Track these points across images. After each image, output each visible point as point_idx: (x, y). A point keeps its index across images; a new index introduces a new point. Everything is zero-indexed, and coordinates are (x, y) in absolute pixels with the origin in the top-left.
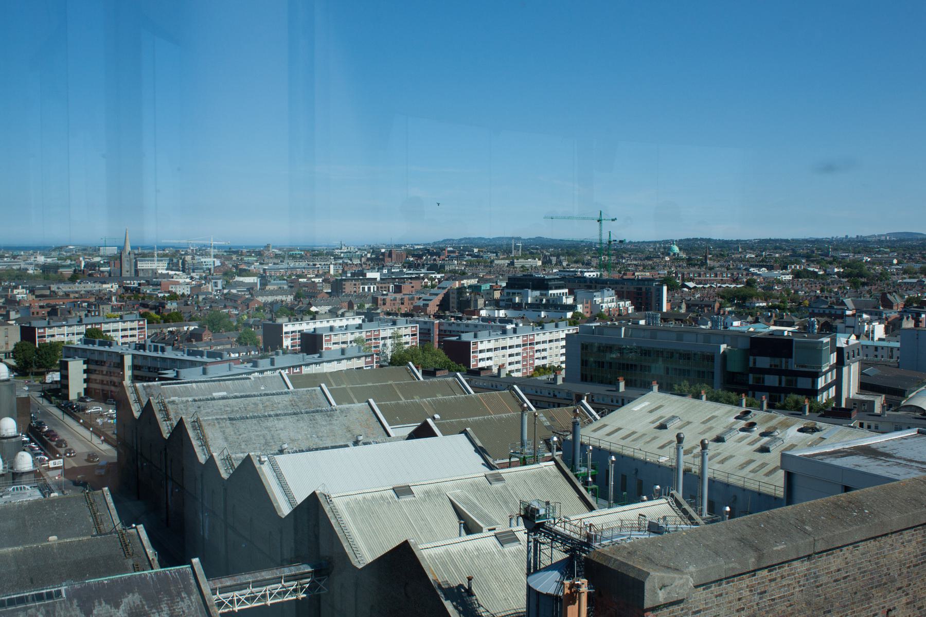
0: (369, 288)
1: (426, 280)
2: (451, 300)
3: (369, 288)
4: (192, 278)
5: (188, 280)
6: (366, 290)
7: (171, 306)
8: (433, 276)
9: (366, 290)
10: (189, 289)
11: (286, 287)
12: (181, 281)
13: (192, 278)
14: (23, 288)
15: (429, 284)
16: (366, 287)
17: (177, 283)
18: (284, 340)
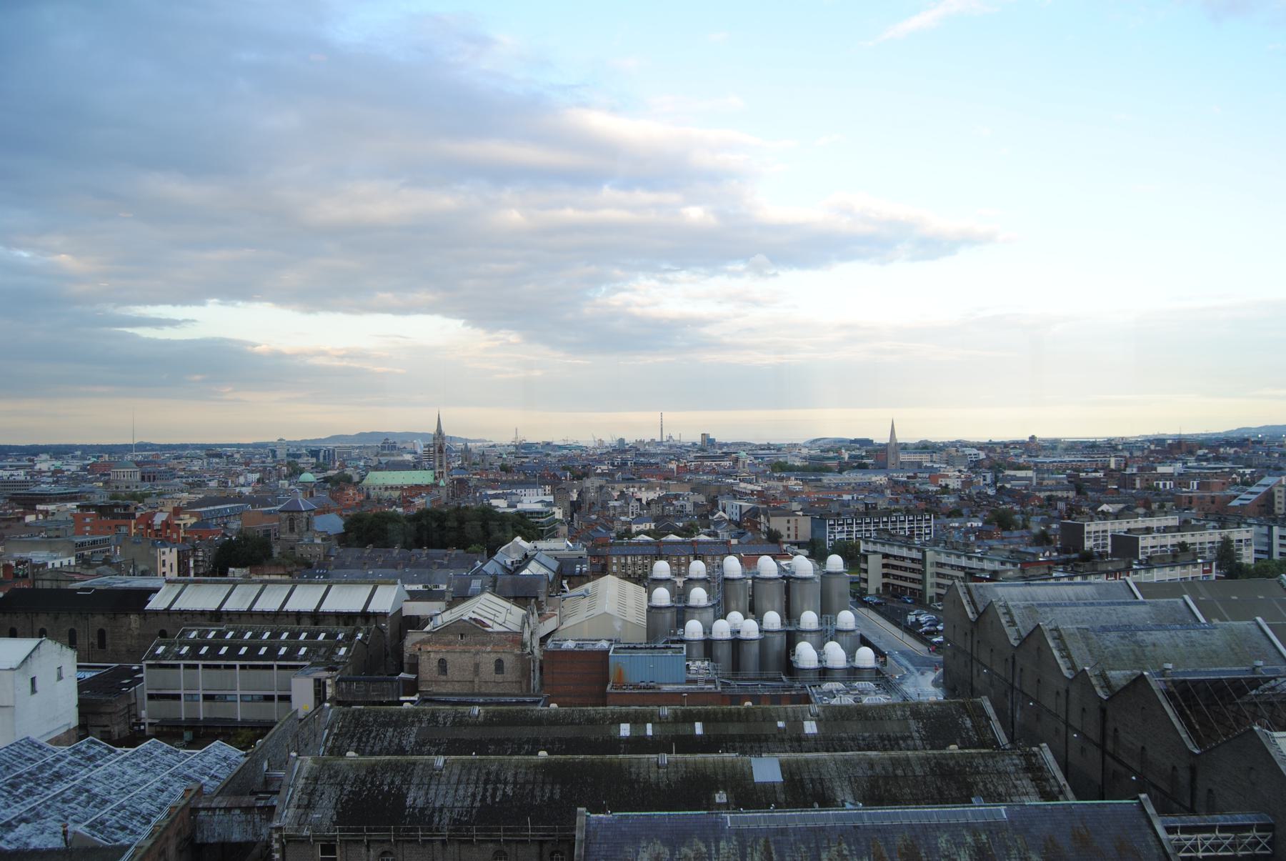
0: (1165, 485)
1: (1234, 476)
2: (1277, 500)
3: (1165, 485)
4: (960, 471)
5: (957, 473)
6: (1161, 486)
7: (950, 501)
8: (1241, 471)
9: (1161, 486)
10: (960, 483)
11: (1066, 482)
12: (950, 474)
13: (960, 471)
14: (796, 479)
15: (1239, 480)
16: (1161, 483)
17: (947, 476)
18: (1085, 539)
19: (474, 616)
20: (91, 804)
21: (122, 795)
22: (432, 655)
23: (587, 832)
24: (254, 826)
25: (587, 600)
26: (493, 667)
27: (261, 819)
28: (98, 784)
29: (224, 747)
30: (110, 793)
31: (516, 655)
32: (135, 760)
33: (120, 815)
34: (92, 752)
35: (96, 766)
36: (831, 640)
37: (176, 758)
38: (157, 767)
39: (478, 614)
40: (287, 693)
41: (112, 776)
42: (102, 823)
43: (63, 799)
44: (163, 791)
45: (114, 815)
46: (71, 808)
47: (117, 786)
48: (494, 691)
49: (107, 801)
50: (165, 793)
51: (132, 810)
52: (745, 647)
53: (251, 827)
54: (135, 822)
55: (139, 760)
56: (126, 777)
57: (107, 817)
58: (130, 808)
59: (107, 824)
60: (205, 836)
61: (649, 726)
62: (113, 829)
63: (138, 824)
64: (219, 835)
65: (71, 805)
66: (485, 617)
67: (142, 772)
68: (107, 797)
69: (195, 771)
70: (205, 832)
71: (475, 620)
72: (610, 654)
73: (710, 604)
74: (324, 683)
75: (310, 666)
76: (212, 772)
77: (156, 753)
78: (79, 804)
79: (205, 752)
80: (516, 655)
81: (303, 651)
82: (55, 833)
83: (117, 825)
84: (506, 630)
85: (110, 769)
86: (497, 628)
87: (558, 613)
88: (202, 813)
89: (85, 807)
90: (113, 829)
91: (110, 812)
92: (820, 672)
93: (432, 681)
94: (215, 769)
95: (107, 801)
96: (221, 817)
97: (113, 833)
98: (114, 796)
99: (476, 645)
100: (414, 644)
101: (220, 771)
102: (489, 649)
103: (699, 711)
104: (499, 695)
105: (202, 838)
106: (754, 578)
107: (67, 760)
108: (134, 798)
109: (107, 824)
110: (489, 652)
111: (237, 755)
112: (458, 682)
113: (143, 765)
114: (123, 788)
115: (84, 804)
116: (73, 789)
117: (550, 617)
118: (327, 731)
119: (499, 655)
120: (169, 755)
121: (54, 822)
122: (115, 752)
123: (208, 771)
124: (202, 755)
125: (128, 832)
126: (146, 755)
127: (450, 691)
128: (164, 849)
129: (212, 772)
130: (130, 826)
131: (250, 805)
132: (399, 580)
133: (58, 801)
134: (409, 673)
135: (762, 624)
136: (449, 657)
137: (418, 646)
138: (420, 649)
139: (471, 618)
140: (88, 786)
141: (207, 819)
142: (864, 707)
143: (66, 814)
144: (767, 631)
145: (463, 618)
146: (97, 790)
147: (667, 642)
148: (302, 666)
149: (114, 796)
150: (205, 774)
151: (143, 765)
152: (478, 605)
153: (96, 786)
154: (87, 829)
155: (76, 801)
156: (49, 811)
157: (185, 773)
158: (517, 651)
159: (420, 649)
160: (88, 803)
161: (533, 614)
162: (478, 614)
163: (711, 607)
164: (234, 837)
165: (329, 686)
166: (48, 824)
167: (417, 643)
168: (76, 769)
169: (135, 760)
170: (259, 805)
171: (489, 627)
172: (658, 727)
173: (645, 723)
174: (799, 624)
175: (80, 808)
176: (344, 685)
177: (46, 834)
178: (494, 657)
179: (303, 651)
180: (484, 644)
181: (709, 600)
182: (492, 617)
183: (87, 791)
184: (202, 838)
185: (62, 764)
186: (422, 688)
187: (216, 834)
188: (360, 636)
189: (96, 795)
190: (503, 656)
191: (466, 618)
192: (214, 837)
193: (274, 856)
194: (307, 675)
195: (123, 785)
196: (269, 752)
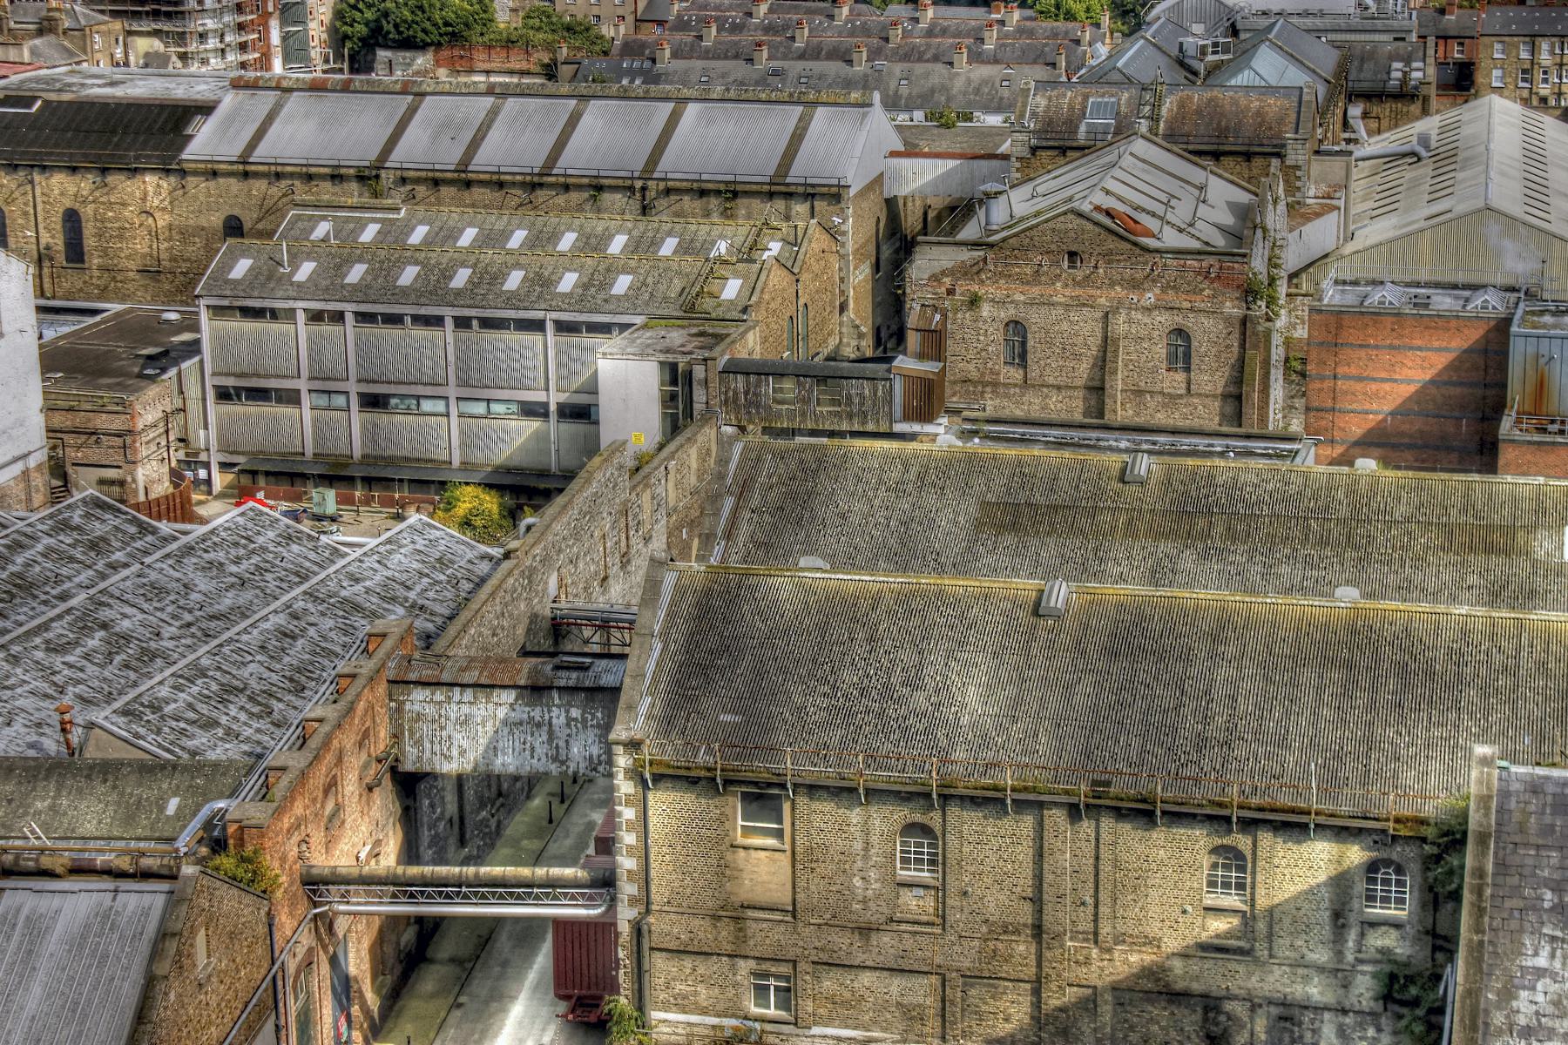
19: (1109, 203)
20: (118, 659)
21: (188, 641)
22: (986, 310)
23: (1501, 810)
24: (551, 733)
25: (1425, 170)
26: (1161, 350)
27: (569, 720)
28: (128, 610)
29: (438, 534)
30: (158, 635)
31: (1228, 320)
32: (212, 555)
33: (195, 689)
34: (98, 529)
35: (114, 567)
37: (312, 555)
38: (269, 577)
39: (1119, 199)
40: (583, 399)
41: (158, 591)
42: (155, 708)
43: (48, 642)
44: (294, 638)
45: (178, 688)
46: (70, 666)
47: (175, 617)
48: (1161, 418)
49: (154, 656)
50: (300, 642)
51: (226, 679)
53: (545, 737)
54: (233, 711)
55: (220, 556)
56: (194, 596)
57: (164, 692)
58: (218, 675)
59: (168, 709)
60: (427, 754)
62: (182, 725)
63: (243, 717)
64: (462, 753)
65: (70, 659)
66: (1137, 208)
67: (232, 586)
68: (153, 645)
69: (368, 591)
70: (427, 745)
71: (1108, 213)
72: (1514, 329)
74: (689, 375)
75: (645, 327)
76: (412, 595)
77: (260, 540)
78: (87, 656)
79: (389, 541)
80: (1228, 320)
81: (622, 284)
82: (39, 725)
83: (191, 715)
84: (1196, 245)
85: (153, 576)
86: (1171, 239)
87: (1342, 204)
88: (419, 694)
89: (102, 666)
90: (182, 725)
91: (171, 681)
93: (985, 384)
94: (418, 588)
95: (154, 656)
96: (465, 709)
97: (183, 732)
98: (171, 644)
99: (1112, 284)
100: (935, 278)
101: (431, 594)
102: (1150, 297)
104: (1174, 432)
105: (420, 759)
107: (40, 547)
108: (226, 650)
109: (168, 709)
110: (1148, 310)
111: (470, 555)
112: (1059, 388)
113: (234, 569)
114: (189, 625)
115: (99, 658)
116: (68, 618)
117: (1318, 215)
118: (729, 503)
119: (1179, 319)
120: (295, 548)
121: (32, 699)
122: (154, 531)
123: (401, 592)
124: (382, 549)
125: (220, 732)
126: (236, 544)
127: (1036, 413)
128: (335, 777)
129: (412, 595)
130: (224, 720)
131: (542, 682)
132: (877, 96)
133: (36, 647)
134: (921, 356)
136: (1035, 319)
137: (947, 280)
138: (950, 292)
139: (1098, 208)
140: (105, 614)
141: (429, 710)
143: (57, 678)
145: (1075, 205)
146: (126, 623)
148: (624, 327)
149: (171, 644)
150: (394, 599)
151: (234, 569)
152: (1117, 172)
153: (125, 616)
154: (122, 720)
155: (78, 651)
156: (19, 671)
157: (344, 593)
158: (1232, 309)
159: (950, 292)
160: (110, 656)
161: (1275, 202)
162: (1119, 199)
164: (499, 761)
165: (699, 382)
166: (20, 703)
167: (943, 273)
168: (64, 571)
169: (212, 555)
170: (562, 683)
171: (1154, 236)
175: (91, 669)
176: (740, 383)
177: (18, 726)
178: (1164, 319)
179: (622, 284)
180: (1135, 285)
182: (1160, 209)
183: (104, 626)
184: (420, 759)
185: (28, 554)
186: (954, 401)
187: (455, 753)
188: (775, 247)
189: (126, 638)
190: (1189, 322)
191: (1086, 207)
192: (448, 758)
193: (620, 815)
194: (642, 355)
195: (188, 617)
196: (560, 551)
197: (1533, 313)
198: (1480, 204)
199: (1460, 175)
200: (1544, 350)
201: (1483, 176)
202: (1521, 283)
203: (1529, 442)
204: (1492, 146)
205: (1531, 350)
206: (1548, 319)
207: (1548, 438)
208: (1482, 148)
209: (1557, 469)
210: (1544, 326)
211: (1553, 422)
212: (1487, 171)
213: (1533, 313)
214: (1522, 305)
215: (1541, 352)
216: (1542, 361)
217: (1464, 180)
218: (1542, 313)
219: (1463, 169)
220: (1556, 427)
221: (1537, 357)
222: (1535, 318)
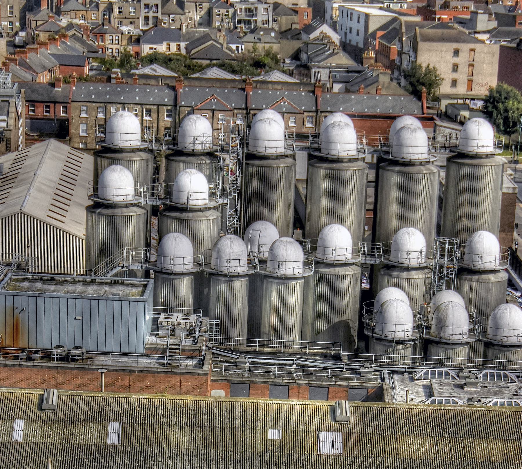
36: (448, 287)
52: (275, 291)
61: (19, 425)
73: (213, 204)
92: (415, 346)
103: (180, 408)
106: (311, 157)
135: (314, 249)
142: (484, 415)
144: (318, 263)
147: (121, 274)
163: (216, 208)
172: (36, 428)
173: (11, 419)
174: (387, 252)
181: (213, 195)
197: (17, 280)
198: (16, 209)
199: (13, 191)
200: (17, 304)
201: (26, 191)
202: (13, 259)
203: (4, 365)
204: (39, 172)
205: (9, 304)
206: (26, 284)
207: (17, 362)
208: (32, 174)
209: (23, 383)
210: (22, 289)
211: (23, 351)
212: (29, 189)
213: (17, 280)
214: (9, 275)
215: (15, 306)
216: (17, 311)
217: (14, 194)
218: (23, 280)
219: (16, 187)
220: (24, 355)
221: (13, 308)
222: (18, 284)
